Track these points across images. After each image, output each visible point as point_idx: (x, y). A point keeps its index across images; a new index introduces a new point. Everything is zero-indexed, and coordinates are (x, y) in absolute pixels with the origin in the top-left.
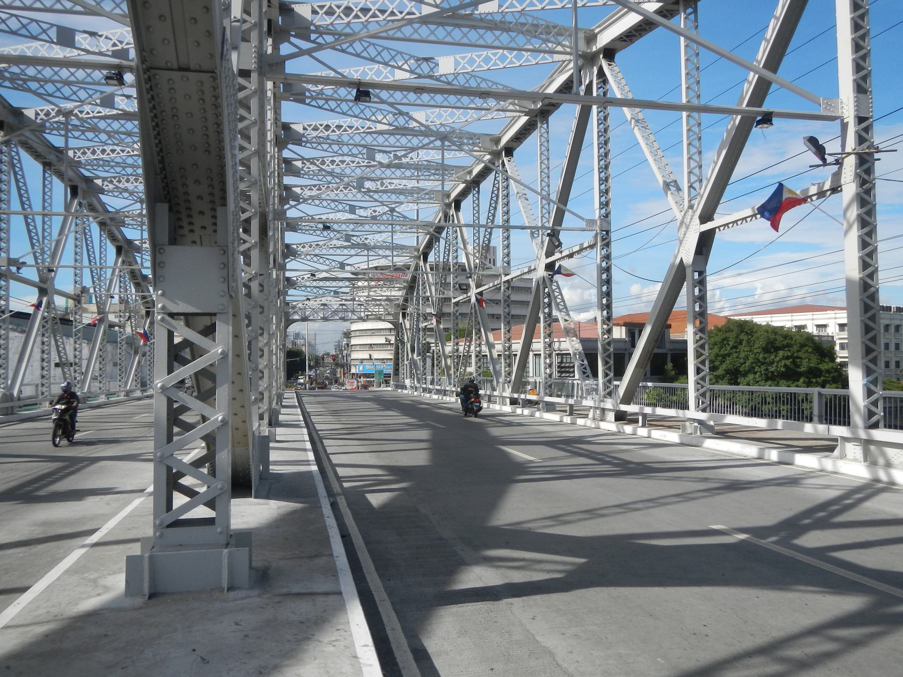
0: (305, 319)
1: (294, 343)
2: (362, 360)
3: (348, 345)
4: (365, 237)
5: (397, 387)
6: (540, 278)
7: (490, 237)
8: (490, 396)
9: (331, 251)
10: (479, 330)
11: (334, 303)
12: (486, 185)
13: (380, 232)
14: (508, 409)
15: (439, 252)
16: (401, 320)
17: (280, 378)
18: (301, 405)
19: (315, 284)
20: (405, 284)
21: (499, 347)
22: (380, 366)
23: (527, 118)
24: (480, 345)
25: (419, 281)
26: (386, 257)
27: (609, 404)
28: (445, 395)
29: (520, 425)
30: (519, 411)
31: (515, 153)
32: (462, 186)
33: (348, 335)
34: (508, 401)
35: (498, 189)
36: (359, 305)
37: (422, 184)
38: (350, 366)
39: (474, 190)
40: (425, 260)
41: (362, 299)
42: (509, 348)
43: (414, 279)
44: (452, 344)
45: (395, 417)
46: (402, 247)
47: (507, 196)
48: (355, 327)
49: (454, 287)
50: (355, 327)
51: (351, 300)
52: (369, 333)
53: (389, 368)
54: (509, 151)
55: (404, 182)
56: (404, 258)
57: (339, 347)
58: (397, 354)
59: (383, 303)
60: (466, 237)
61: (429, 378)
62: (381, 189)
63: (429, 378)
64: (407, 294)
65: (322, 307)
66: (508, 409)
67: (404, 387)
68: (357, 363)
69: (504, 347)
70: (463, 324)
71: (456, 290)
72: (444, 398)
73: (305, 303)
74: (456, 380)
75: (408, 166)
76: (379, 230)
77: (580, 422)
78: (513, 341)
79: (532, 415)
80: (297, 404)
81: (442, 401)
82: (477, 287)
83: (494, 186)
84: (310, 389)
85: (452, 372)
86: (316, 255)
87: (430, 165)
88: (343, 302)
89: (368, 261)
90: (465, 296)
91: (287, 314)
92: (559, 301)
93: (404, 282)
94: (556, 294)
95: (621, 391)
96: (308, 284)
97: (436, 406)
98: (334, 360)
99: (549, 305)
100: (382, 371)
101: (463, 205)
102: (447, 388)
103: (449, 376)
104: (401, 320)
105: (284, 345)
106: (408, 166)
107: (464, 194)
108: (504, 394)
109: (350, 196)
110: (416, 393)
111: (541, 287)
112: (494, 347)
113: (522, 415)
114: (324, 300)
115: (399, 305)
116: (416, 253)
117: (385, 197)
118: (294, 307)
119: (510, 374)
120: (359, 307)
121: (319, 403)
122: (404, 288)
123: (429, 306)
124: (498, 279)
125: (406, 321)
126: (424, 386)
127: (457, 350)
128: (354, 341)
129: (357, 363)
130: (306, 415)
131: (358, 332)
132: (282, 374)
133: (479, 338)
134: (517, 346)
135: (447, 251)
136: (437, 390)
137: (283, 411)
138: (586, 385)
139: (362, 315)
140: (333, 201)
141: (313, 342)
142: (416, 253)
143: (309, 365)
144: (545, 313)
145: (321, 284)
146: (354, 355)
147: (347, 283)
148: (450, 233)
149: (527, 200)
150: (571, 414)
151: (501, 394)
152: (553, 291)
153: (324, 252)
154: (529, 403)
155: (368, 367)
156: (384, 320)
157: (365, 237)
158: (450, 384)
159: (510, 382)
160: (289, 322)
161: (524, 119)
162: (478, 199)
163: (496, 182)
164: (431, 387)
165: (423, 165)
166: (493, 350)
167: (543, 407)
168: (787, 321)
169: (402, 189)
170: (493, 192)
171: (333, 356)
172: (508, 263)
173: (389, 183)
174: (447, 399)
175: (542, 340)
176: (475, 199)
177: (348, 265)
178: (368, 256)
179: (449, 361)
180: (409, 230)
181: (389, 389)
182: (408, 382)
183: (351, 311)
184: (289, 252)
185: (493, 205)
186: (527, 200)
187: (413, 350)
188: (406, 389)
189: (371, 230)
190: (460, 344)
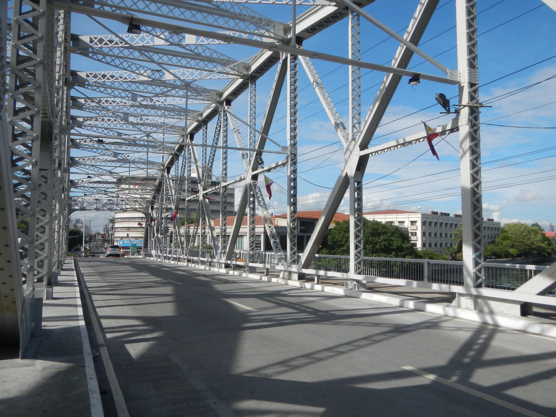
0: (83, 209)
1: (75, 226)
2: (122, 238)
3: (113, 227)
4: (128, 154)
5: (146, 255)
6: (248, 184)
7: (213, 157)
8: (210, 262)
9: (104, 164)
10: (204, 219)
11: (104, 198)
12: (212, 125)
13: (139, 152)
14: (223, 271)
15: (178, 167)
16: (150, 211)
17: (62, 249)
18: (77, 268)
19: (91, 185)
20: (154, 188)
21: (217, 231)
22: (134, 242)
23: (242, 80)
24: (204, 228)
25: (163, 186)
26: (143, 169)
27: (294, 268)
28: (179, 261)
29: (234, 282)
30: (231, 272)
31: (232, 103)
32: (196, 124)
33: (113, 221)
34: (223, 265)
35: (220, 126)
36: (121, 200)
37: (167, 121)
38: (114, 241)
39: (204, 126)
40: (168, 172)
41: (124, 197)
42: (225, 230)
43: (160, 184)
44: (185, 228)
45: (146, 277)
46: (153, 163)
47: (226, 131)
48: (118, 216)
49: (188, 190)
50: (118, 216)
51: (116, 197)
52: (127, 220)
53: (140, 243)
54: (228, 102)
55: (157, 118)
56: (154, 170)
57: (106, 229)
58: (146, 234)
59: (138, 199)
60: (197, 157)
61: (168, 249)
62: (140, 122)
63: (168, 249)
64: (155, 193)
65: (96, 201)
66: (223, 271)
67: (151, 256)
68: (119, 239)
69: (222, 229)
70: (194, 216)
71: (189, 192)
72: (179, 263)
73: (84, 198)
74: (187, 251)
75: (159, 108)
76: (137, 150)
77: (274, 280)
78: (227, 227)
79: (240, 275)
80: (74, 268)
81: (177, 265)
82: (204, 190)
83: (217, 124)
84: (85, 256)
85: (185, 246)
86: (92, 166)
87: (175, 109)
88: (111, 198)
89: (129, 171)
90: (195, 196)
91: (70, 205)
92: (260, 200)
93: (153, 186)
94: (259, 195)
95: (303, 260)
96: (86, 185)
97: (174, 268)
98: (103, 237)
99: (253, 202)
100: (136, 245)
101: (195, 136)
102: (181, 257)
103: (183, 248)
104: (150, 211)
105: (67, 227)
106: (159, 108)
107: (197, 129)
108: (221, 261)
109: (118, 126)
110: (159, 260)
111: (248, 190)
112: (214, 230)
113: (233, 275)
114: (97, 196)
115: (148, 202)
116: (162, 167)
117: (142, 128)
118: (75, 201)
119: (224, 248)
120: (122, 202)
121: (91, 267)
122: (153, 190)
123: (170, 203)
124: (218, 185)
125: (154, 212)
126: (165, 255)
127: (189, 231)
128: (117, 225)
129: (119, 239)
130: (80, 275)
131: (120, 219)
132: (64, 247)
133: (204, 223)
134: (230, 230)
135: (184, 166)
136: (174, 258)
137: (62, 273)
138: (278, 256)
139: (124, 207)
140: (106, 129)
141: (88, 225)
142: (162, 167)
143: (85, 241)
144: (250, 207)
145: (95, 185)
146: (117, 235)
147: (114, 186)
148: (186, 154)
149: (240, 133)
150: (267, 275)
151: (219, 261)
152: (257, 193)
153: (98, 163)
154: (238, 267)
155: (125, 242)
156: (139, 211)
157: (128, 154)
158: (183, 254)
159: (224, 253)
160: (71, 211)
161: (240, 81)
162: (206, 133)
163: (219, 122)
164: (170, 256)
165: (170, 108)
166: (213, 232)
167: (248, 270)
169: (155, 124)
170: (216, 128)
171: (102, 234)
172: (226, 174)
173: (146, 119)
174: (181, 264)
175: (248, 226)
176: (204, 132)
177: (115, 173)
178: (129, 167)
179: (182, 238)
180: (158, 152)
181: (141, 257)
182: (153, 252)
183: (116, 204)
184: (73, 162)
185: (217, 137)
186: (240, 133)
187: (158, 232)
188: (152, 257)
189: (132, 150)
190: (191, 228)
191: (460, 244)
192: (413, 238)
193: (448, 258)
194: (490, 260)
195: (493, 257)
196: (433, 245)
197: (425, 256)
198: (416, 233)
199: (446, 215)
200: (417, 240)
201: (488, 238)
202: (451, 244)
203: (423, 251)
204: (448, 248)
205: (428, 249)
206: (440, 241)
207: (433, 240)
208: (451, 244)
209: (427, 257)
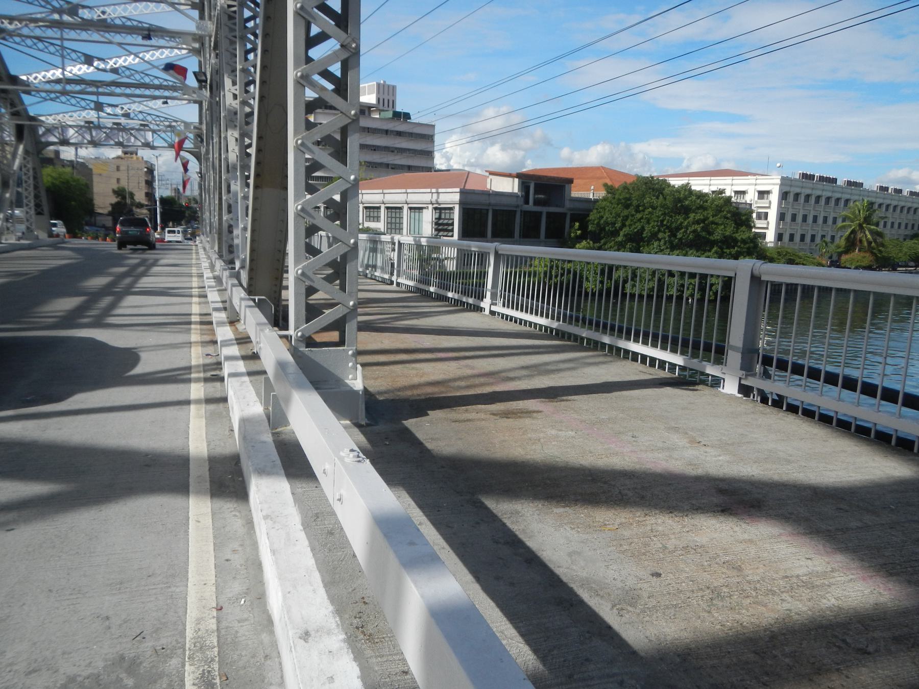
168: (749, 184)
191: (852, 236)
192: (759, 223)
193: (824, 262)
194: (904, 269)
195: (912, 264)
196: (797, 238)
197: (780, 257)
198: (766, 214)
199: (829, 182)
200: (767, 228)
201: (906, 227)
202: (833, 237)
203: (776, 248)
204: (826, 244)
205: (786, 246)
206: (812, 230)
207: (799, 228)
208: (833, 237)
209: (784, 260)
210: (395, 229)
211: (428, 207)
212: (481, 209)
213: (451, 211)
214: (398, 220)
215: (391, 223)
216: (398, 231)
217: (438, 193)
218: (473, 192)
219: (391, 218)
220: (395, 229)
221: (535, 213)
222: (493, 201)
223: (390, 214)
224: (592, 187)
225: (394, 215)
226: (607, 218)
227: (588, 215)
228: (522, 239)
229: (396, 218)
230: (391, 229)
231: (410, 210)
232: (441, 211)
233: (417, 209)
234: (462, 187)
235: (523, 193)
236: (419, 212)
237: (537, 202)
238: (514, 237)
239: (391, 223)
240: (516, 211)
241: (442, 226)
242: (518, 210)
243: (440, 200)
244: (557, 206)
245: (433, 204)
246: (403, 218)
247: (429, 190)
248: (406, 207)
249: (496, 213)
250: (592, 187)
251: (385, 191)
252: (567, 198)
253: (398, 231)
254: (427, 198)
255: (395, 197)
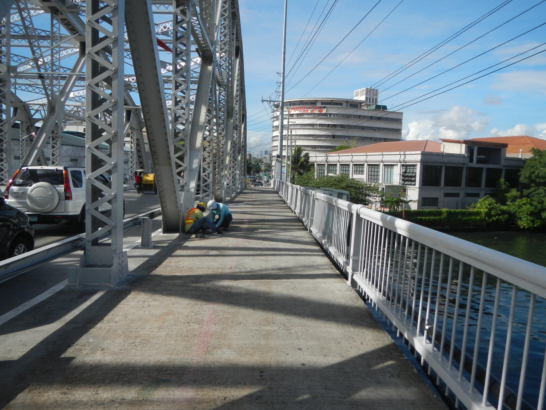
210: (374, 179)
211: (397, 164)
212: (437, 166)
213: (414, 167)
214: (376, 174)
215: (371, 175)
216: (375, 181)
217: (405, 154)
218: (431, 154)
219: (371, 171)
220: (374, 179)
221: (478, 168)
222: (446, 160)
223: (370, 169)
224: (521, 150)
225: (373, 169)
226: (538, 173)
227: (519, 171)
228: (467, 188)
229: (374, 172)
230: (371, 179)
231: (385, 166)
232: (407, 167)
233: (390, 166)
234: (423, 151)
235: (469, 155)
236: (391, 168)
237: (479, 161)
238: (461, 186)
239: (371, 175)
240: (462, 168)
241: (407, 178)
242: (465, 166)
243: (407, 159)
244: (494, 164)
245: (401, 162)
246: (379, 172)
247: (398, 153)
248: (382, 164)
249: (447, 168)
250: (521, 150)
251: (368, 154)
252: (503, 158)
253: (375, 181)
254: (397, 158)
255: (374, 157)
